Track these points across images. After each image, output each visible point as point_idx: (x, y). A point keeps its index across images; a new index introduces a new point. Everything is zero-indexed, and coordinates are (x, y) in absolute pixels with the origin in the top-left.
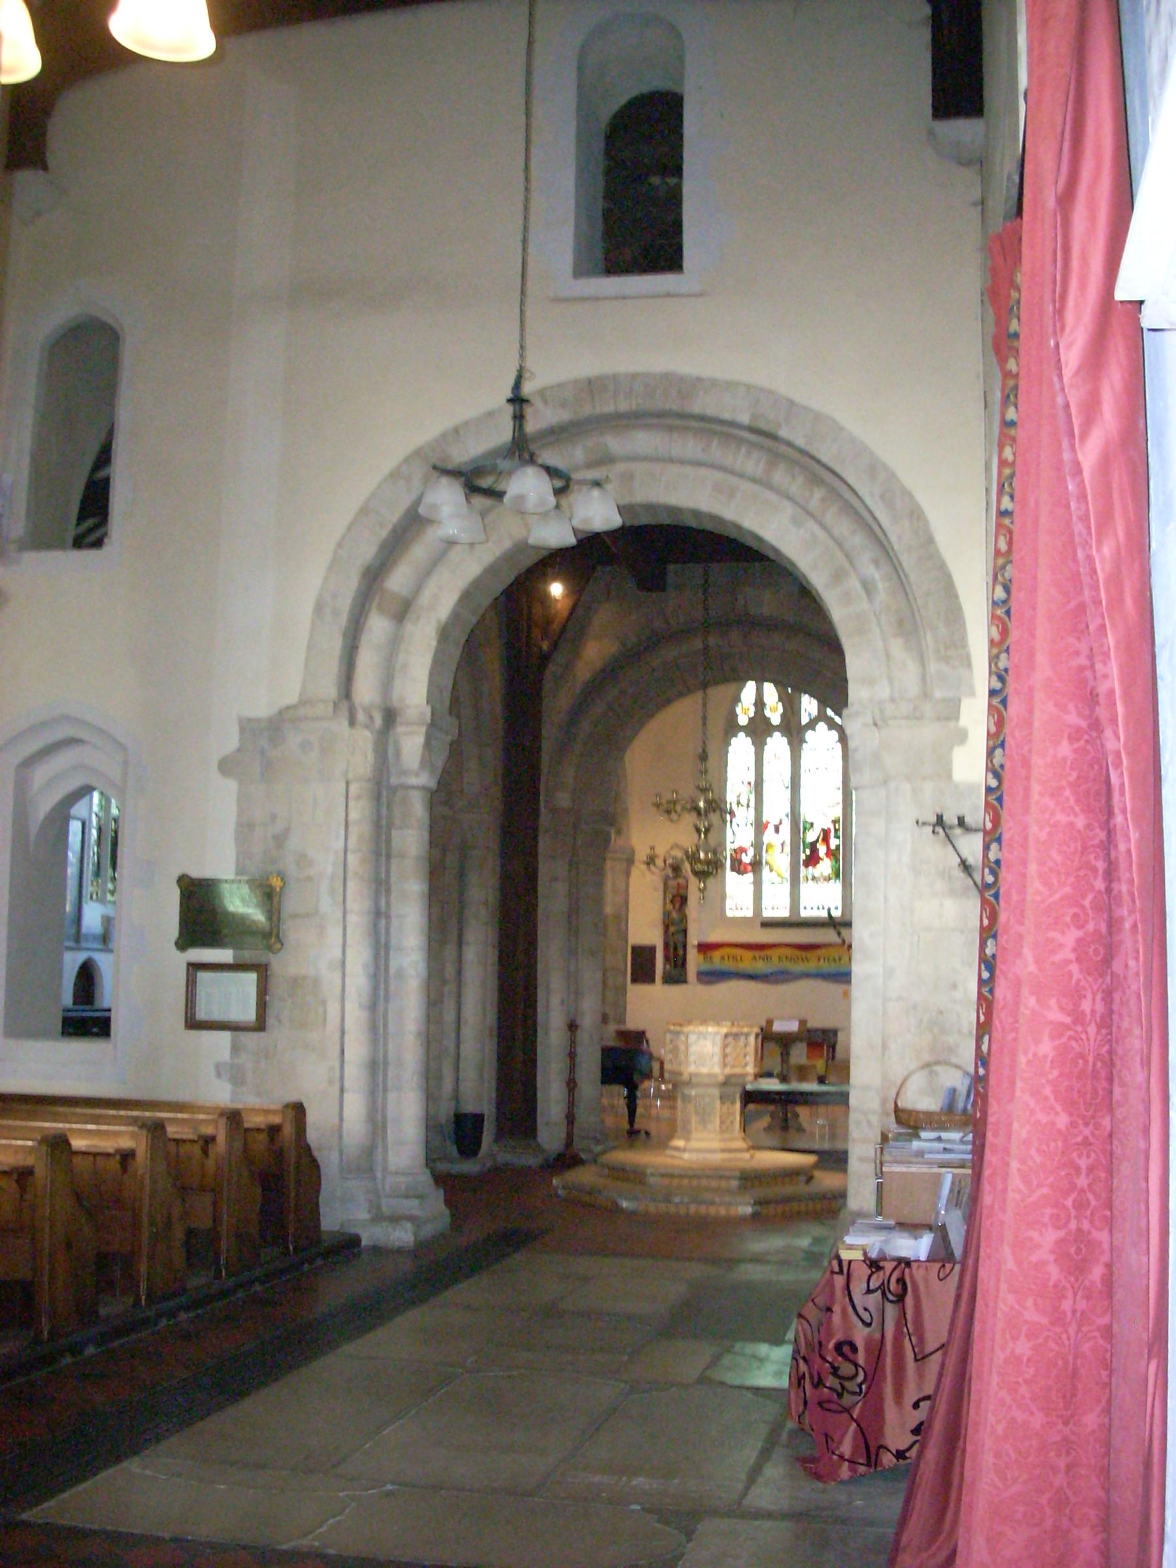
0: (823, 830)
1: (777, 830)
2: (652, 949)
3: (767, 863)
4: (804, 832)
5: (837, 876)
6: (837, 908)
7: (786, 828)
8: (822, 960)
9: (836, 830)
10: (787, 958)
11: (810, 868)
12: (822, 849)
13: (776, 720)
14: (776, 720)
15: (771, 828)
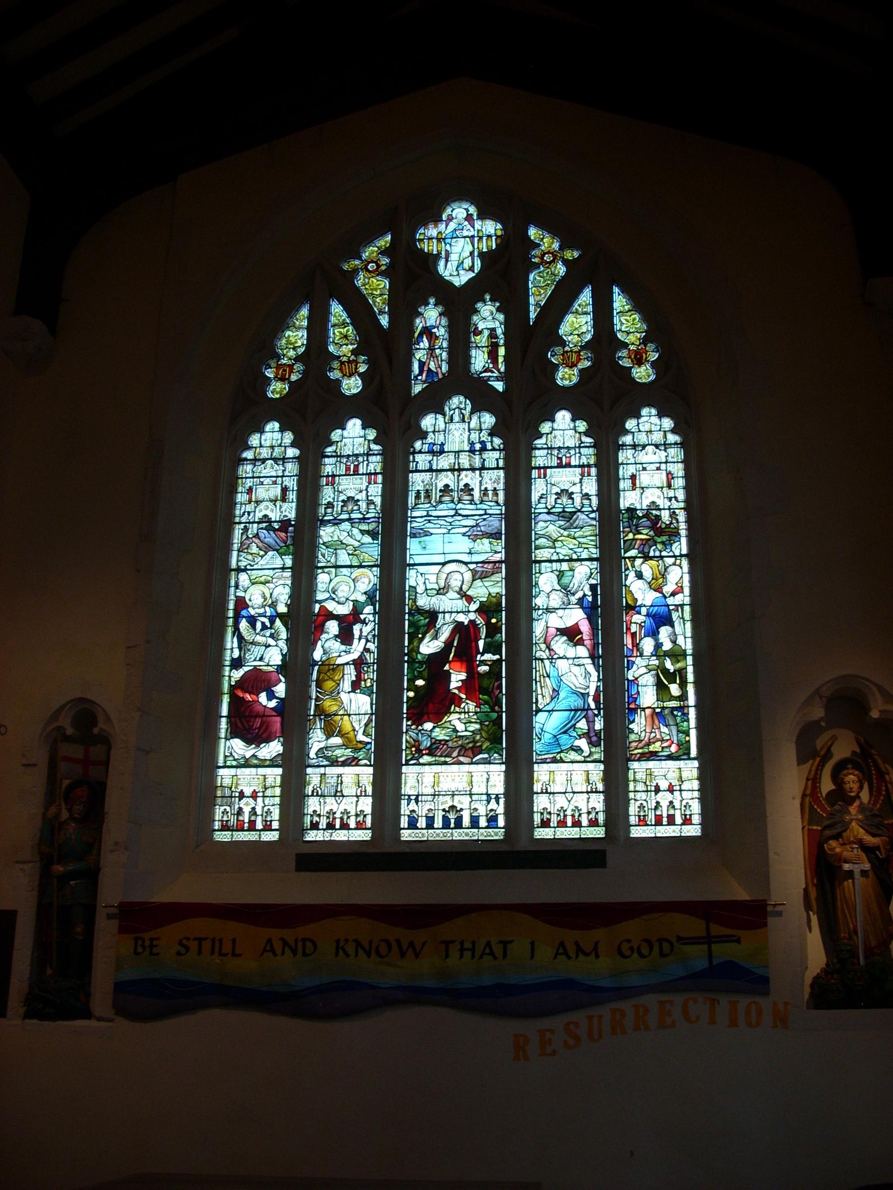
0: (459, 627)
1: (345, 637)
2: (11, 915)
3: (320, 711)
4: (412, 637)
5: (495, 740)
6: (492, 820)
7: (365, 629)
8: (454, 950)
9: (493, 630)
10: (358, 944)
11: (428, 726)
12: (457, 679)
13: (352, 386)
14: (352, 386)
15: (333, 627)
